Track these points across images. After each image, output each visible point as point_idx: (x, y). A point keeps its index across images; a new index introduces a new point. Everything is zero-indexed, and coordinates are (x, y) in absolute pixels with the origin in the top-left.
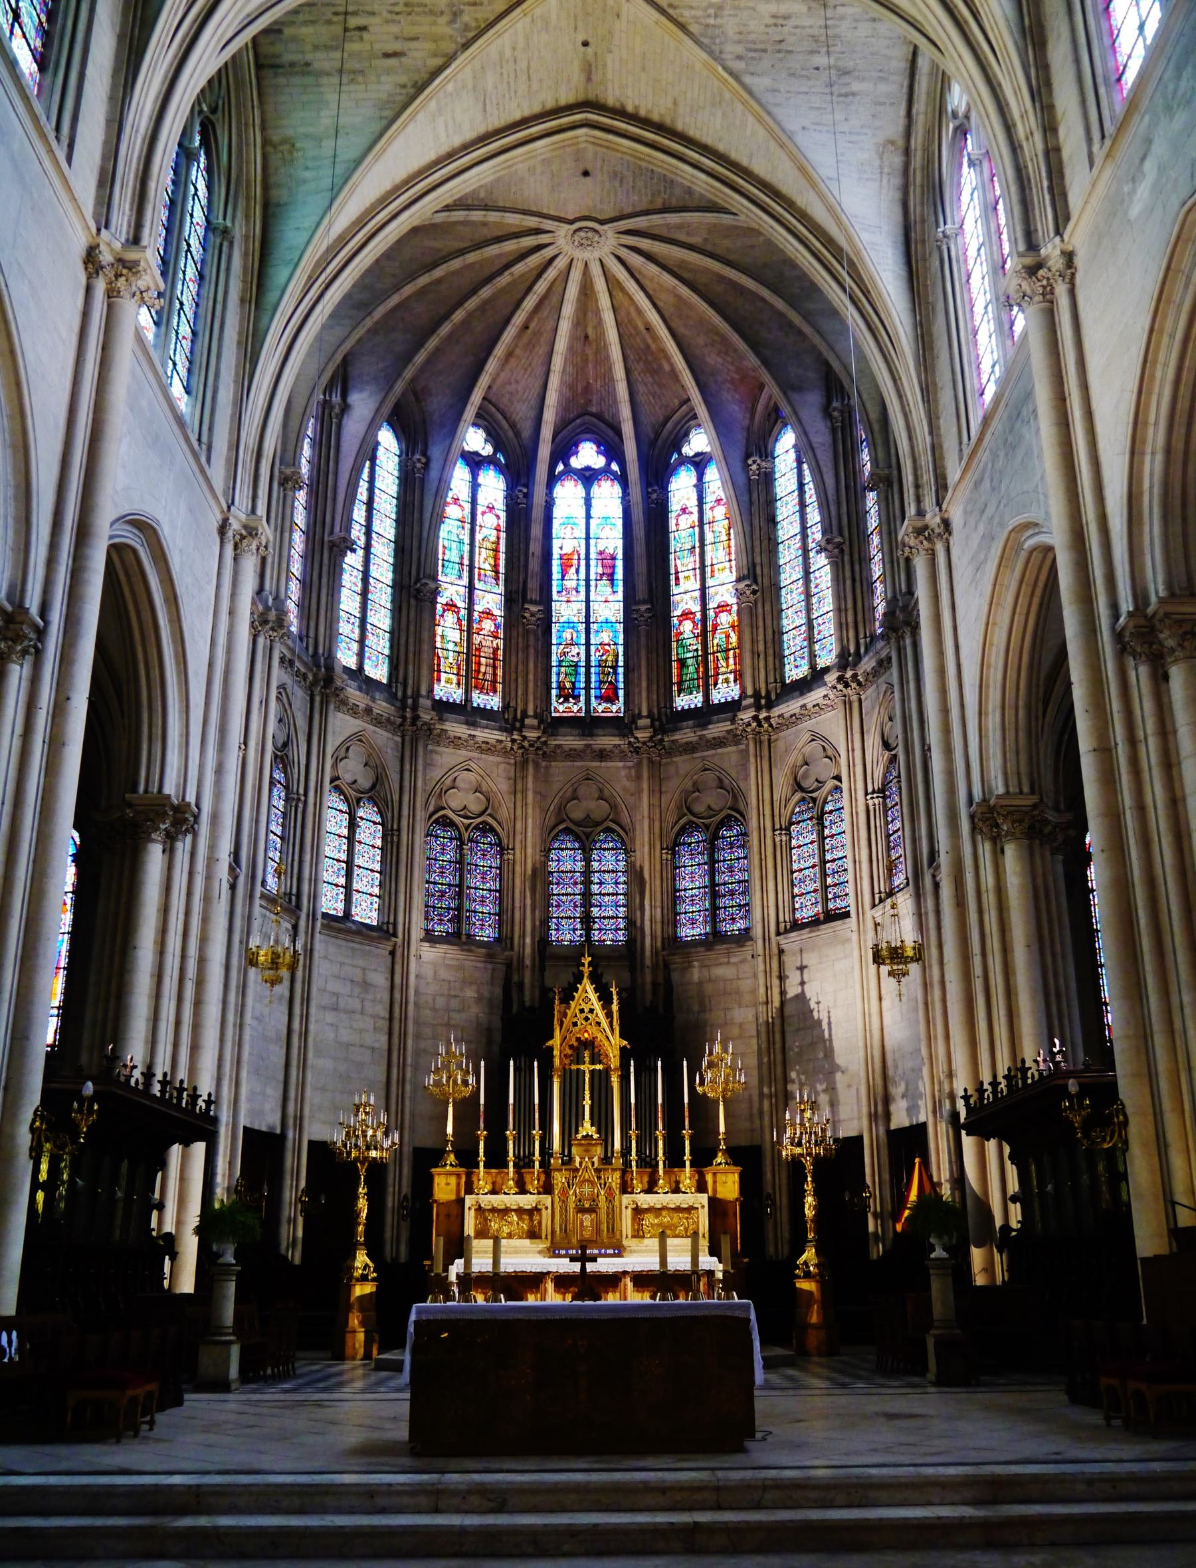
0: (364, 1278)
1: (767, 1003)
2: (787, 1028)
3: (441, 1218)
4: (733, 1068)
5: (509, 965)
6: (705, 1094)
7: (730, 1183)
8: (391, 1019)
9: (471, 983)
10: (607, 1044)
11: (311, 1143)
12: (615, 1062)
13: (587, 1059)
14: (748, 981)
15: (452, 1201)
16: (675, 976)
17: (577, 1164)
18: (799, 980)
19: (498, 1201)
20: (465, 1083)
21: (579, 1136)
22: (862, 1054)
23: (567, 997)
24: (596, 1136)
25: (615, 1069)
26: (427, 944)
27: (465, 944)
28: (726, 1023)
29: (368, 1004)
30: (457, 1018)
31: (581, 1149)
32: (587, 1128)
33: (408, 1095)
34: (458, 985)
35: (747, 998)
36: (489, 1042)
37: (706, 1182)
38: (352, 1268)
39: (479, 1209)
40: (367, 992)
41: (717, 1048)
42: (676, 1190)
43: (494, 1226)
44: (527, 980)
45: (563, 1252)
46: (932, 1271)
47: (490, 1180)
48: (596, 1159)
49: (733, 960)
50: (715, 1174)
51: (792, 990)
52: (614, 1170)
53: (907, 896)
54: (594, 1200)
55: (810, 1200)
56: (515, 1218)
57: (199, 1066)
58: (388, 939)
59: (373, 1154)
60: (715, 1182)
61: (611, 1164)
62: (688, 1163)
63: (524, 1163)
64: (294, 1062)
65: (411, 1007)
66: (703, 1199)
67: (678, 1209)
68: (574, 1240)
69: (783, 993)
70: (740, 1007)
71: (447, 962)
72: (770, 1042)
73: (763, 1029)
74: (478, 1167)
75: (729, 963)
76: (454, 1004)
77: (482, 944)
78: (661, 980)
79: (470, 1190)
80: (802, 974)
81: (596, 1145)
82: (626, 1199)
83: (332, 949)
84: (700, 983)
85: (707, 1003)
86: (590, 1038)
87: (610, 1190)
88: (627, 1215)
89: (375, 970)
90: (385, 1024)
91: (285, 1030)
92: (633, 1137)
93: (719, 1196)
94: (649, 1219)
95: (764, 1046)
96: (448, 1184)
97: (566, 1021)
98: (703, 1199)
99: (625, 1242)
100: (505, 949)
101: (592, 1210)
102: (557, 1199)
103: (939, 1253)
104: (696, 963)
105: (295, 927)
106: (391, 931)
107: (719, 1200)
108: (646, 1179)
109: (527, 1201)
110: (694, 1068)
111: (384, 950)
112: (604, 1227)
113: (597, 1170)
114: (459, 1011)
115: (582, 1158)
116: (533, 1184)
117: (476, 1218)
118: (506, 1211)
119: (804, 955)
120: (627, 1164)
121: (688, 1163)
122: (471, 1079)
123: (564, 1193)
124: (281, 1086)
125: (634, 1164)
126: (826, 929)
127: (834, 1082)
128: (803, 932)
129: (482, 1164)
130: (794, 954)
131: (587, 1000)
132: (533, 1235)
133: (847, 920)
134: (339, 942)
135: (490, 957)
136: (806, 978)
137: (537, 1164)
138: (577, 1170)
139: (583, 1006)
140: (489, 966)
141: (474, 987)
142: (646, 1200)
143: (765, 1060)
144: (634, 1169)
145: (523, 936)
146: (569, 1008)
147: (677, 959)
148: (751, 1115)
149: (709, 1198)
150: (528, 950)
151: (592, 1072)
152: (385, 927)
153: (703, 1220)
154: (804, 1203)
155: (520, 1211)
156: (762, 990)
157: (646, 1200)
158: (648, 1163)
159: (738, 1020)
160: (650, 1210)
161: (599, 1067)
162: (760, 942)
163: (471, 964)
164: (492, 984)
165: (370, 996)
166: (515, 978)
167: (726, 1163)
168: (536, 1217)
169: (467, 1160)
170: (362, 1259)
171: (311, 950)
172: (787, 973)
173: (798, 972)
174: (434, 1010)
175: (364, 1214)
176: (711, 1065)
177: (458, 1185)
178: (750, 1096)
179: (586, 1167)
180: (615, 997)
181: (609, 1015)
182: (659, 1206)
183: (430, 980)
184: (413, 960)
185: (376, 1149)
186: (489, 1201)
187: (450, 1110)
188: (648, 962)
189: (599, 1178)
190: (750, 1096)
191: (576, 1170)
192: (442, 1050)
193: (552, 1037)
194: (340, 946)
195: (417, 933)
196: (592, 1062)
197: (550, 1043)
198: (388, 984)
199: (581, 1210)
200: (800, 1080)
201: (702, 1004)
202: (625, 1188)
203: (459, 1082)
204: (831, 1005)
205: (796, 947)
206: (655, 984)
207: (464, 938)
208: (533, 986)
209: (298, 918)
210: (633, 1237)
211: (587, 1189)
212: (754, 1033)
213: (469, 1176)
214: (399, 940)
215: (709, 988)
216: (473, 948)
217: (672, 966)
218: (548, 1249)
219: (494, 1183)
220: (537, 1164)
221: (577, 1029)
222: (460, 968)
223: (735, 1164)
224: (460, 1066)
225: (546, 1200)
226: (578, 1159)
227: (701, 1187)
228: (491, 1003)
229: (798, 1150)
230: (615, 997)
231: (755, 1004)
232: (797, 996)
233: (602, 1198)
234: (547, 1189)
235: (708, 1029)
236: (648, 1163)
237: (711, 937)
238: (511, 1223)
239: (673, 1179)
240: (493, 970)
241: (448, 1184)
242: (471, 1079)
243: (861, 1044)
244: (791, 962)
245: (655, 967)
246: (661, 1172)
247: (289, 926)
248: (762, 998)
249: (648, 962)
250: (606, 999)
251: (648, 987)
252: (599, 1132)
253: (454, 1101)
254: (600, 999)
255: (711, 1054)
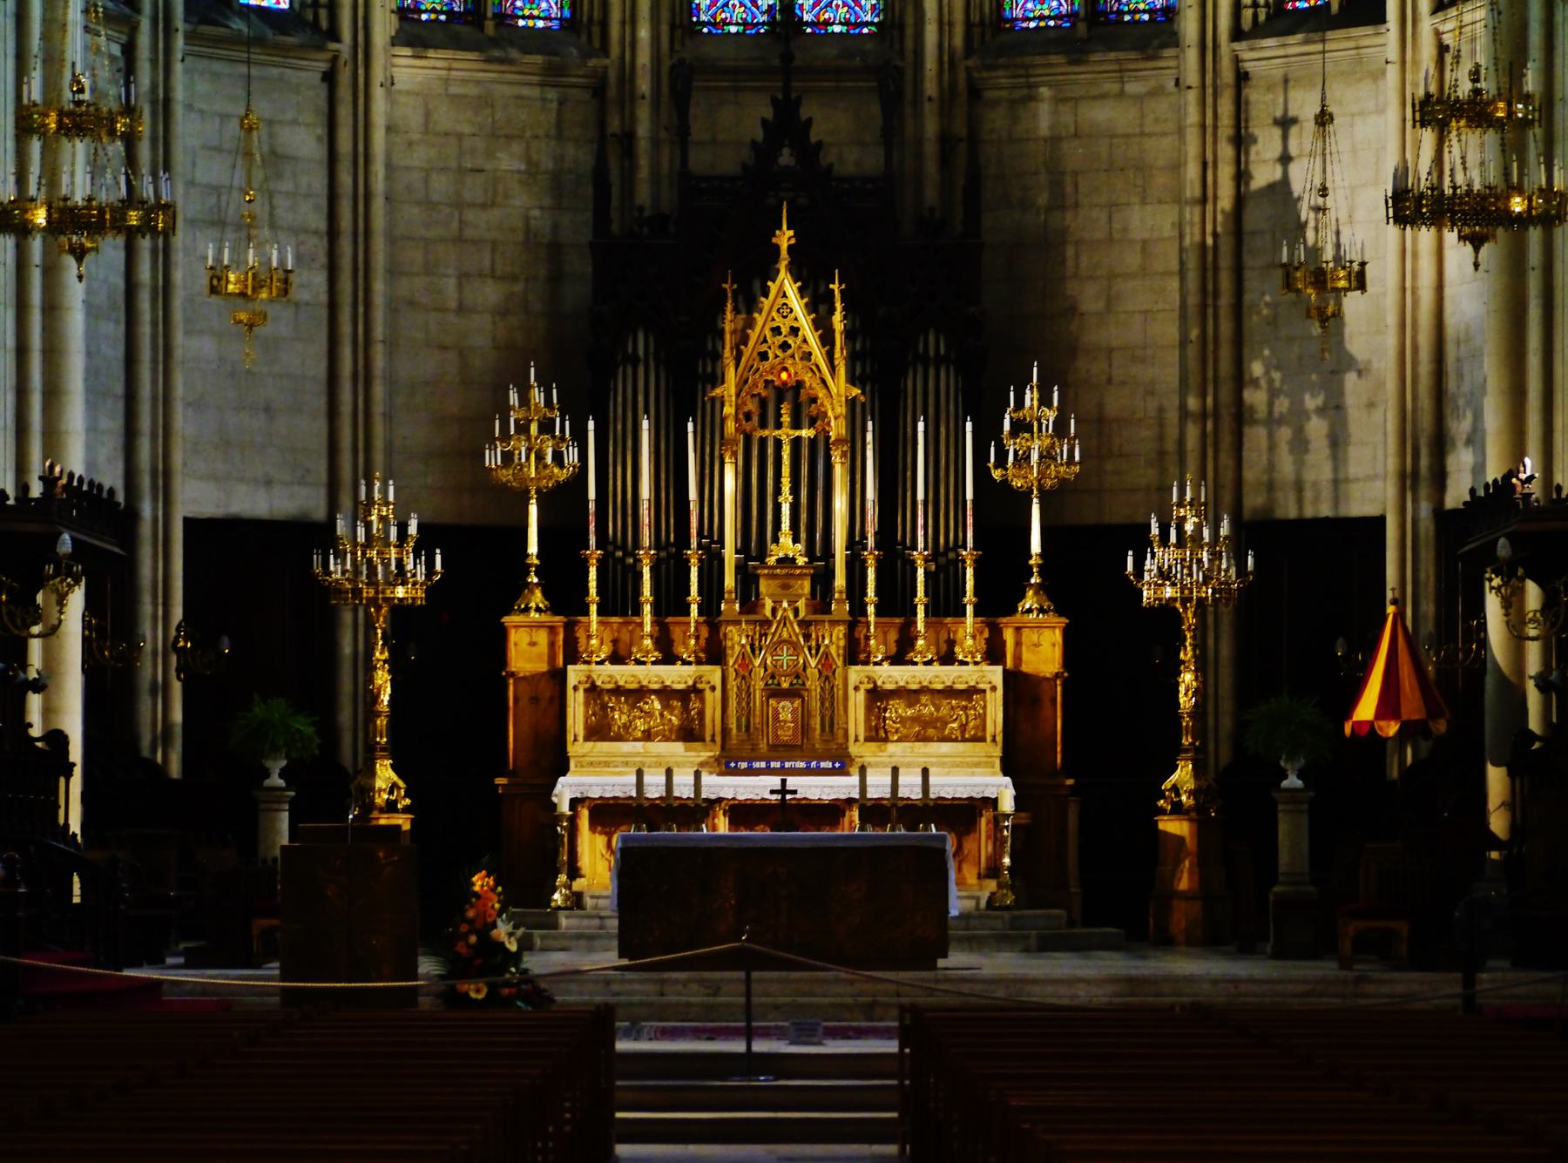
0: (391, 807)
1: (1203, 201)
2: (1248, 261)
3: (524, 702)
4: (1060, 428)
5: (598, 89)
6: (1005, 482)
7: (1046, 647)
8: (333, 233)
9: (509, 138)
10: (821, 394)
11: (187, 522)
12: (837, 429)
13: (786, 419)
14: (1167, 143)
15: (543, 674)
16: (996, 120)
17: (768, 612)
18: (1275, 149)
19: (625, 674)
20: (558, 458)
21: (771, 561)
22: (1391, 340)
23: (748, 304)
24: (801, 561)
25: (839, 441)
26: (407, 51)
27: (495, 42)
28: (1110, 240)
29: (281, 203)
30: (482, 222)
31: (774, 583)
32: (787, 546)
33: (378, 408)
34: (480, 144)
35: (1161, 180)
36: (556, 278)
37: (1004, 643)
38: (370, 789)
39: (593, 690)
40: (279, 176)
41: (1032, 398)
42: (948, 658)
43: (619, 718)
44: (643, 130)
45: (744, 765)
46: (1280, 807)
47: (608, 637)
48: (801, 604)
49: (1133, 88)
50: (1018, 630)
51: (1263, 174)
52: (834, 623)
53: (1481, 14)
54: (799, 674)
55: (1187, 678)
56: (657, 705)
57: (63, 427)
58: (320, 48)
59: (400, 592)
60: (1018, 644)
61: (828, 611)
62: (970, 609)
63: (670, 602)
64: (145, 354)
65: (378, 205)
66: (995, 674)
67: (949, 692)
68: (763, 746)
69: (1241, 176)
70: (1143, 202)
71: (454, 90)
72: (1208, 293)
73: (1192, 263)
74: (586, 613)
75: (1121, 94)
76: (474, 189)
77: (533, 41)
78: (960, 129)
79: (573, 656)
80: (1285, 138)
81: (801, 576)
82: (856, 673)
83: (202, 86)
84: (1055, 140)
85: (1069, 189)
86: (792, 383)
87: (826, 662)
88: (857, 701)
89: (295, 122)
90: (319, 246)
91: (120, 283)
92: (871, 561)
93: (1024, 668)
94: (897, 710)
95: (1193, 300)
96: (533, 644)
97: (747, 352)
98: (995, 674)
99: (853, 749)
100: (587, 54)
101: (791, 694)
102: (732, 675)
103: (1292, 781)
104: (1044, 91)
105: (129, 50)
106: (324, 24)
107: (1026, 676)
108: (893, 636)
109: (677, 675)
110: (988, 433)
111: (309, 73)
112: (816, 723)
113: (802, 623)
114: (484, 206)
115: (777, 603)
116: (688, 646)
117: (587, 704)
118: (638, 694)
119: (1294, 94)
120: (858, 608)
121: (970, 609)
122: (571, 456)
123: (744, 663)
124: (121, 405)
125: (871, 609)
126: (1341, 42)
127: (1340, 392)
128: (1291, 40)
129: (593, 608)
130: (1270, 88)
131: (784, 310)
132: (689, 733)
133: (1382, 29)
134: (217, 66)
135: (553, 74)
136: (1293, 150)
137: (694, 608)
138: (767, 623)
139: (779, 321)
140: (552, 94)
141: (517, 148)
142: (890, 675)
143: (1194, 334)
144: (872, 618)
145: (631, 20)
146: (750, 324)
147: (1002, 78)
148: (1162, 454)
149: (1006, 673)
150: (644, 58)
151: (796, 442)
152: (310, 16)
153: (995, 711)
154: (1177, 684)
155: (665, 693)
156: (1192, 171)
157: (890, 675)
158: (895, 601)
159: (1138, 230)
160: (901, 693)
161: (806, 433)
162: (1192, 55)
163: (509, 91)
164: (560, 136)
165: (286, 185)
166: (614, 124)
167: (1041, 610)
168: (695, 705)
169: (565, 600)
170: (385, 774)
171: (168, 101)
172: (1255, 130)
173: (1277, 133)
174: (428, 204)
175: (385, 698)
176: (1020, 427)
177: (552, 645)
178: (1161, 410)
179: (785, 618)
180: (838, 306)
181: (827, 339)
182: (914, 687)
183: (416, 136)
184: (378, 93)
185: (404, 583)
186: (609, 674)
187: (533, 510)
188: (930, 87)
189: (807, 637)
190: (1161, 410)
191: (767, 623)
192: (513, 398)
193: (717, 379)
194: (216, 76)
195: (383, 26)
196: (796, 425)
197: (718, 391)
198: (320, 152)
199: (775, 693)
200: (1271, 381)
201: (1056, 186)
202: (855, 653)
203: (549, 459)
204: (1343, 217)
205: (1275, 70)
206: (945, 139)
207: (490, 27)
208: (655, 142)
209: (134, 30)
210: (868, 739)
211: (785, 657)
212: (1174, 265)
213: (570, 628)
214: (345, 47)
215: (1074, 154)
216: (514, 53)
217: (990, 94)
218: (717, 760)
219: (615, 642)
220: (694, 608)
221: (767, 364)
222: (484, 102)
223: (1060, 612)
224: (546, 427)
225: (713, 674)
226: (769, 604)
227: (994, 654)
228: (558, 186)
229: (1169, 592)
230: (838, 306)
231: (1179, 200)
232: (1271, 187)
233: (812, 672)
234: (714, 653)
235: (1070, 251)
236: (895, 601)
237: (1082, 28)
238: (649, 714)
239: (943, 636)
240: (561, 103)
241: (533, 644)
242: (571, 456)
243: (1392, 319)
244: (1263, 104)
245: (947, 99)
246: (920, 626)
247: (116, 50)
248: (1192, 190)
249: (930, 87)
250: (819, 305)
251: (931, 148)
252: (810, 552)
253: (538, 491)
254: (811, 308)
255: (1020, 404)
